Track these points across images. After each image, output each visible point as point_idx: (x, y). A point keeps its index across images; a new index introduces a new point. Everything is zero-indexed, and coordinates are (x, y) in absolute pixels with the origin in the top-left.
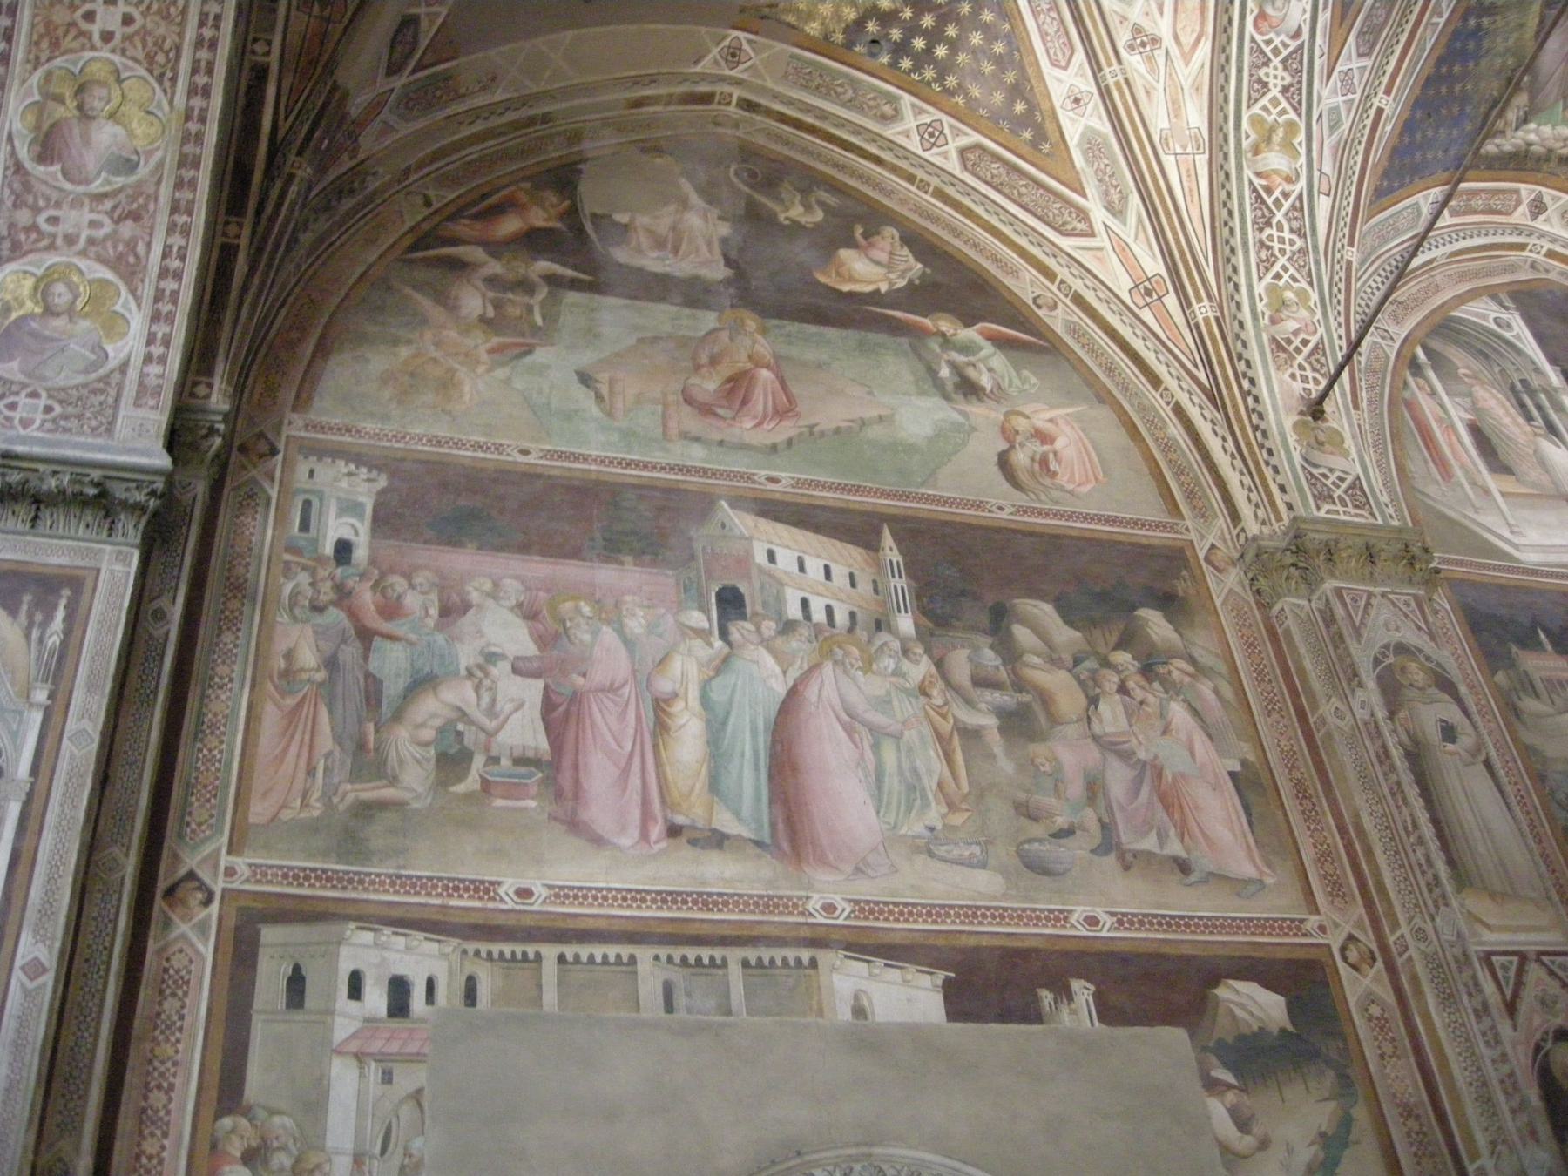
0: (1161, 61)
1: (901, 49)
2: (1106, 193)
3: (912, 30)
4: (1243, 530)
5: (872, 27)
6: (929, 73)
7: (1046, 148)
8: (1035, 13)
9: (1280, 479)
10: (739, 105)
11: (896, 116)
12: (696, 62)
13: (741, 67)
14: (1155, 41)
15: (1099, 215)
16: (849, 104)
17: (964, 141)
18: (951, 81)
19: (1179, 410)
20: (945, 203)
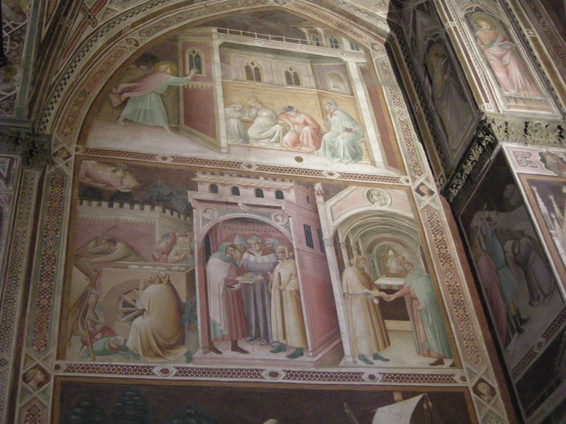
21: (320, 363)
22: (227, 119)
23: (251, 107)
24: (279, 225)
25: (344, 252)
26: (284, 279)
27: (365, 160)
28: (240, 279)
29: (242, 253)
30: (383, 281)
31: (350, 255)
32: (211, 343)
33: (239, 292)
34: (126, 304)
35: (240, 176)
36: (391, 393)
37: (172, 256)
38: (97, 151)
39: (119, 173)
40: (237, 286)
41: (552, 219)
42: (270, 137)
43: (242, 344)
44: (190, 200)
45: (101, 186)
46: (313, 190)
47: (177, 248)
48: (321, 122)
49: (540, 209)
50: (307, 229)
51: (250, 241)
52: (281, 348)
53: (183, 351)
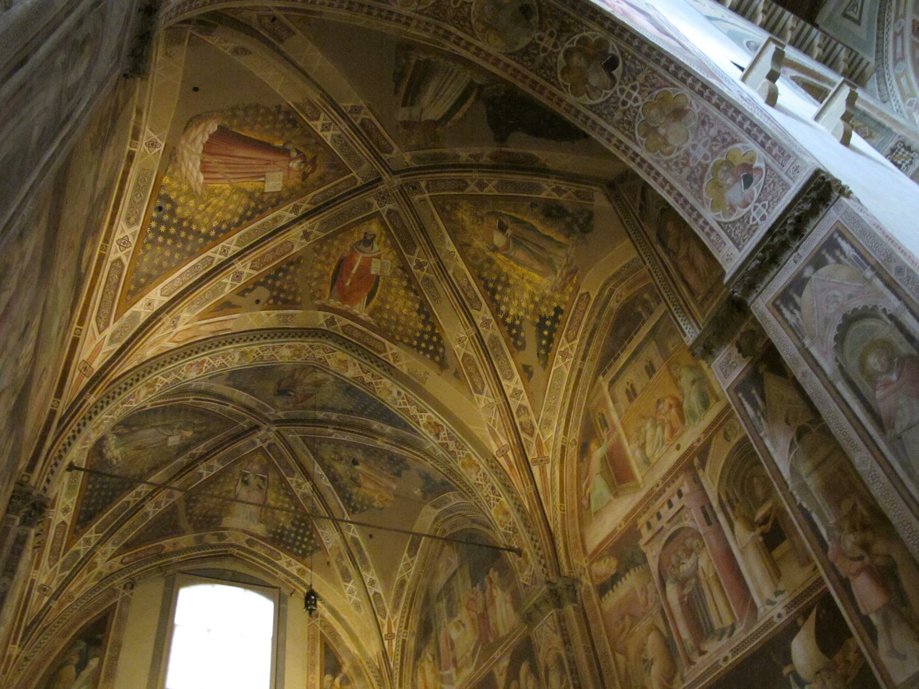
0: (168, 331)
1: (160, 221)
2: (117, 332)
3: (168, 225)
4: (29, 477)
5: (168, 206)
6: (151, 236)
7: (129, 297)
8: (180, 276)
9: (50, 476)
10: (130, 151)
11: (130, 225)
12: (151, 129)
13: (147, 148)
14: (175, 326)
15: (108, 332)
16: (132, 201)
17: (124, 259)
18: (149, 247)
19: (53, 413)
20: (98, 260)
21: (748, 628)
22: (634, 455)
23: (640, 428)
24: (687, 523)
25: (729, 509)
26: (706, 571)
27: (712, 401)
28: (686, 591)
29: (678, 568)
30: (760, 514)
31: (733, 508)
32: (689, 659)
33: (688, 604)
34: (645, 661)
35: (656, 500)
36: (795, 622)
37: (651, 604)
38: (595, 552)
39: (607, 561)
40: (686, 599)
41: (759, 418)
42: (658, 445)
43: (705, 647)
44: (643, 549)
45: (604, 579)
46: (695, 468)
47: (650, 596)
48: (676, 394)
49: (748, 416)
50: (703, 508)
51: (679, 553)
52: (722, 632)
53: (678, 677)
